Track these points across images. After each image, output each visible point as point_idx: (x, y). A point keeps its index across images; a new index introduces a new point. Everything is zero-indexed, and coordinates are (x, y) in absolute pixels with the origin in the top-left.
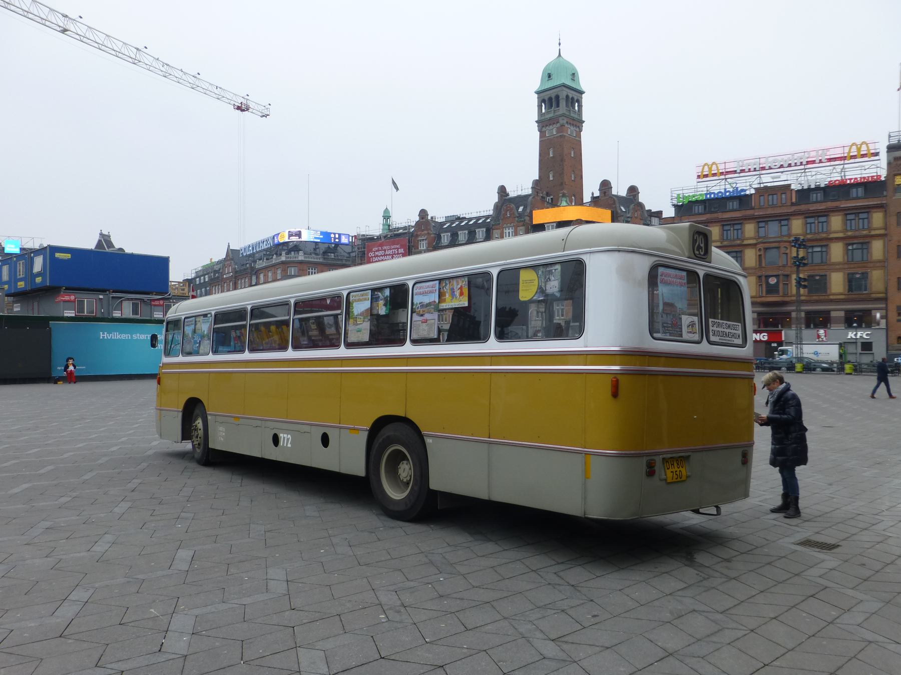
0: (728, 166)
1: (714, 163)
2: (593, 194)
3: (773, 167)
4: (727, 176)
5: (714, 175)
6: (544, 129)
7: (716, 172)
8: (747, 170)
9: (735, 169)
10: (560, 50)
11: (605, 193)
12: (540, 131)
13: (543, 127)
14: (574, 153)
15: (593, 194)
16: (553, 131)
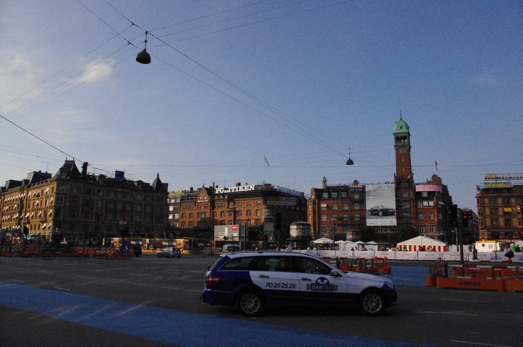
0: (497, 175)
1: (492, 174)
2: (427, 180)
3: (514, 177)
4: (497, 179)
5: (492, 178)
6: (398, 149)
7: (493, 177)
8: (505, 178)
9: (500, 177)
10: (401, 118)
11: (435, 180)
12: (396, 150)
13: (398, 148)
14: (404, 159)
15: (427, 180)
16: (401, 151)
